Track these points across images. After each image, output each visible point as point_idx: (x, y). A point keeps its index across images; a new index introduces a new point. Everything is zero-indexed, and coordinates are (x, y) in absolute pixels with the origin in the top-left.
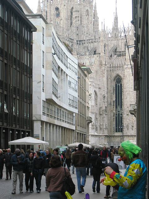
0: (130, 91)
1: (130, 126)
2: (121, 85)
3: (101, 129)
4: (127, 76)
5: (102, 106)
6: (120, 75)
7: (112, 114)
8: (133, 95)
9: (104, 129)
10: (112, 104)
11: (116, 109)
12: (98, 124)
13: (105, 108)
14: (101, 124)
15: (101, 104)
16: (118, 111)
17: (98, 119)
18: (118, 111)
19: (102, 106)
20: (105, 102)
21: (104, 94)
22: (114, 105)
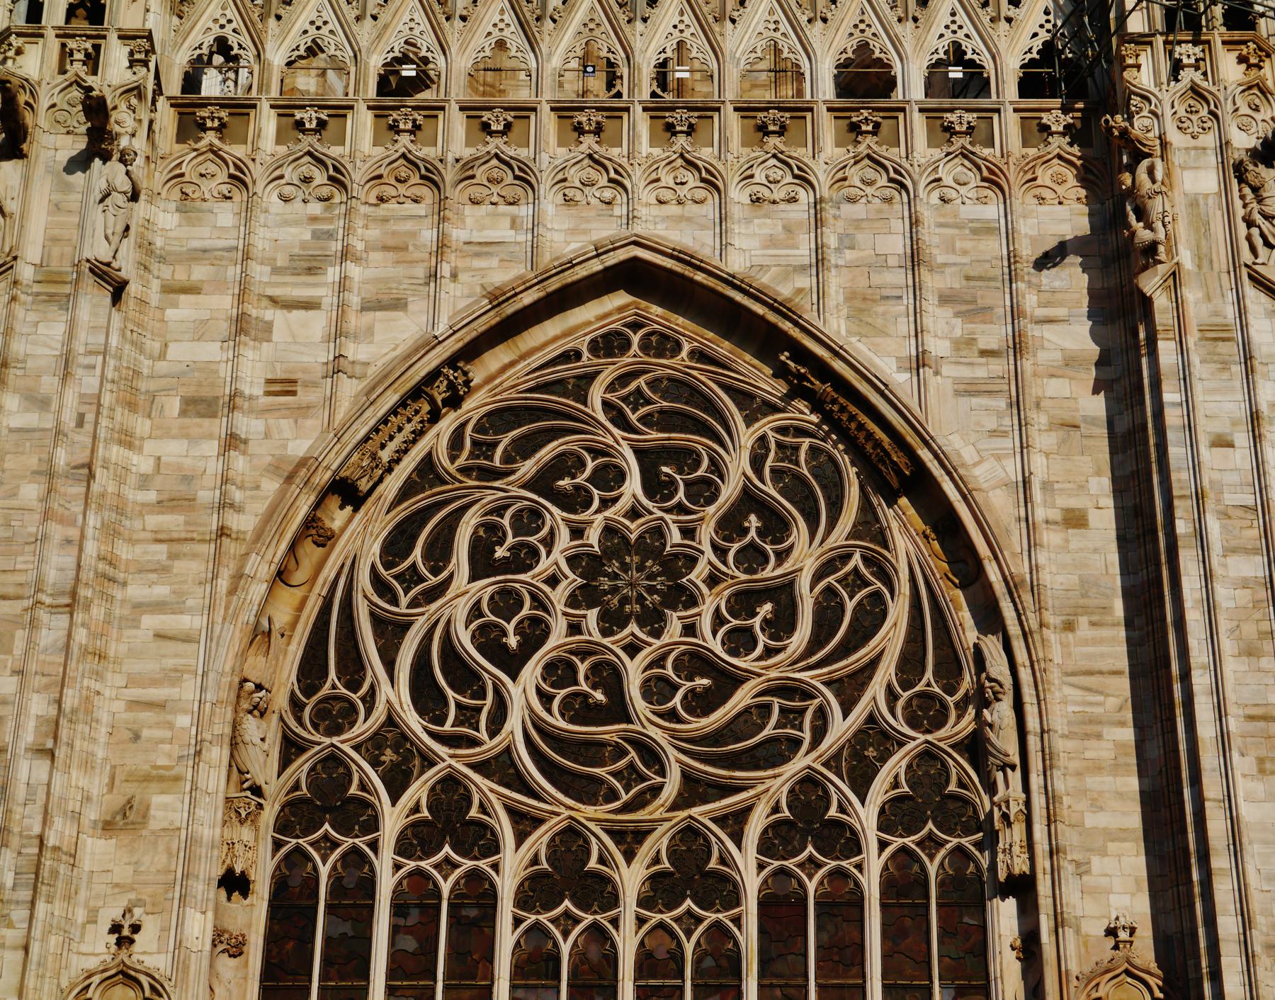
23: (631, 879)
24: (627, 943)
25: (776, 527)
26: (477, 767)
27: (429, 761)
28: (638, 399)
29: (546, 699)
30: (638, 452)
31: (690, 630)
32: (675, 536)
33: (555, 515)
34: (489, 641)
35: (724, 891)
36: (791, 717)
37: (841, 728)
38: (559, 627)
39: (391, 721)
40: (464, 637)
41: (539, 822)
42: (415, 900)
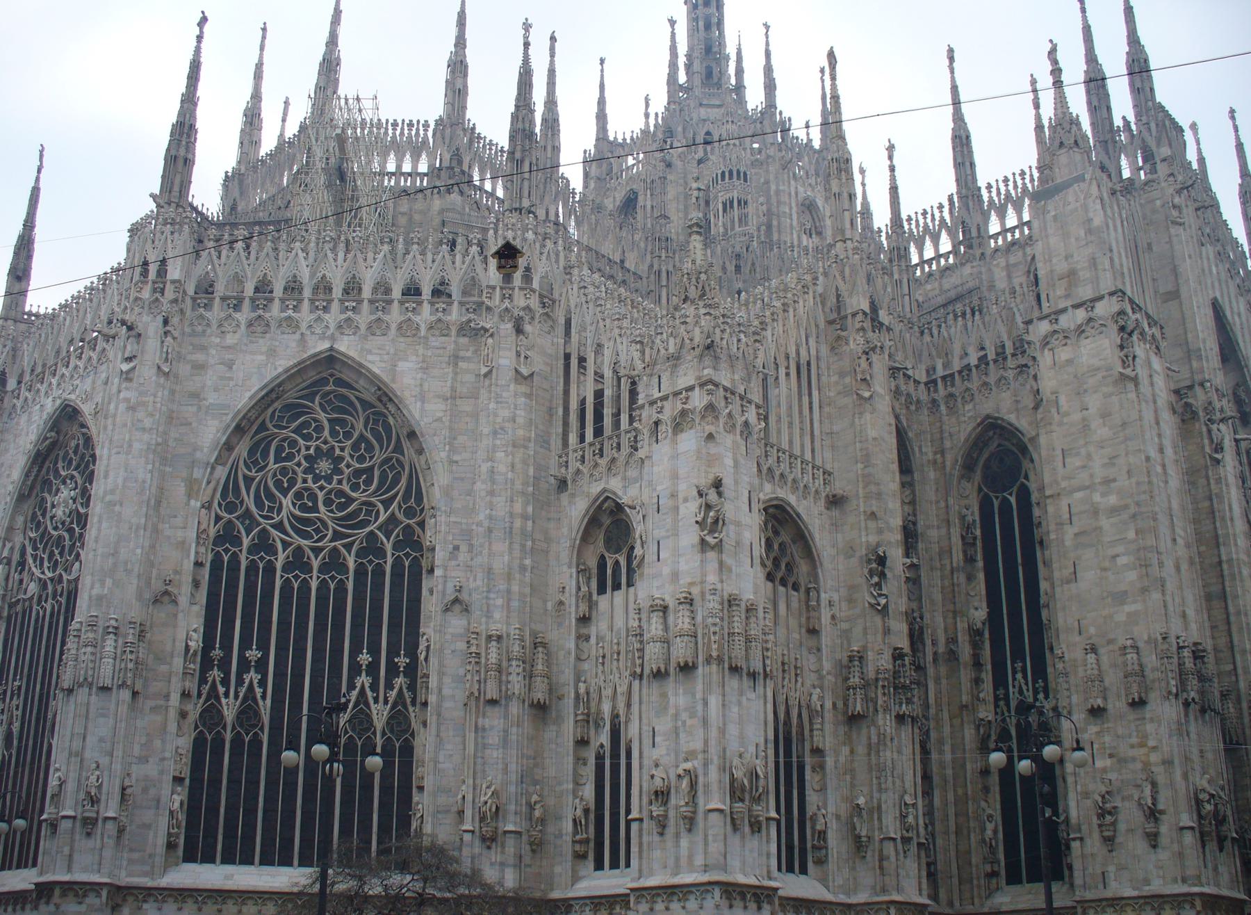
0: (1095, 512)
1: (1129, 816)
2: (1024, 494)
3: (859, 845)
4: (1063, 400)
5: (865, 648)
6: (1012, 418)
7: (969, 734)
8: (1131, 535)
9: (889, 849)
10: (965, 651)
11: (1001, 692)
12: (831, 808)
13: (885, 662)
14: (861, 801)
15: (857, 631)
16: (1013, 704)
17: (829, 761)
18: (1013, 704)
19: (865, 648)
20: (884, 612)
21: (878, 545)
22: (977, 665)
23: (316, 564)
24: (314, 584)
25: (370, 448)
26: (273, 526)
27: (259, 524)
28: (330, 402)
29: (294, 505)
30: (329, 420)
31: (340, 482)
32: (338, 452)
33: (301, 442)
34: (278, 484)
35: (343, 568)
36: (369, 513)
37: (382, 518)
38: (300, 480)
39: (248, 509)
40: (271, 484)
41: (291, 544)
42: (252, 568)
